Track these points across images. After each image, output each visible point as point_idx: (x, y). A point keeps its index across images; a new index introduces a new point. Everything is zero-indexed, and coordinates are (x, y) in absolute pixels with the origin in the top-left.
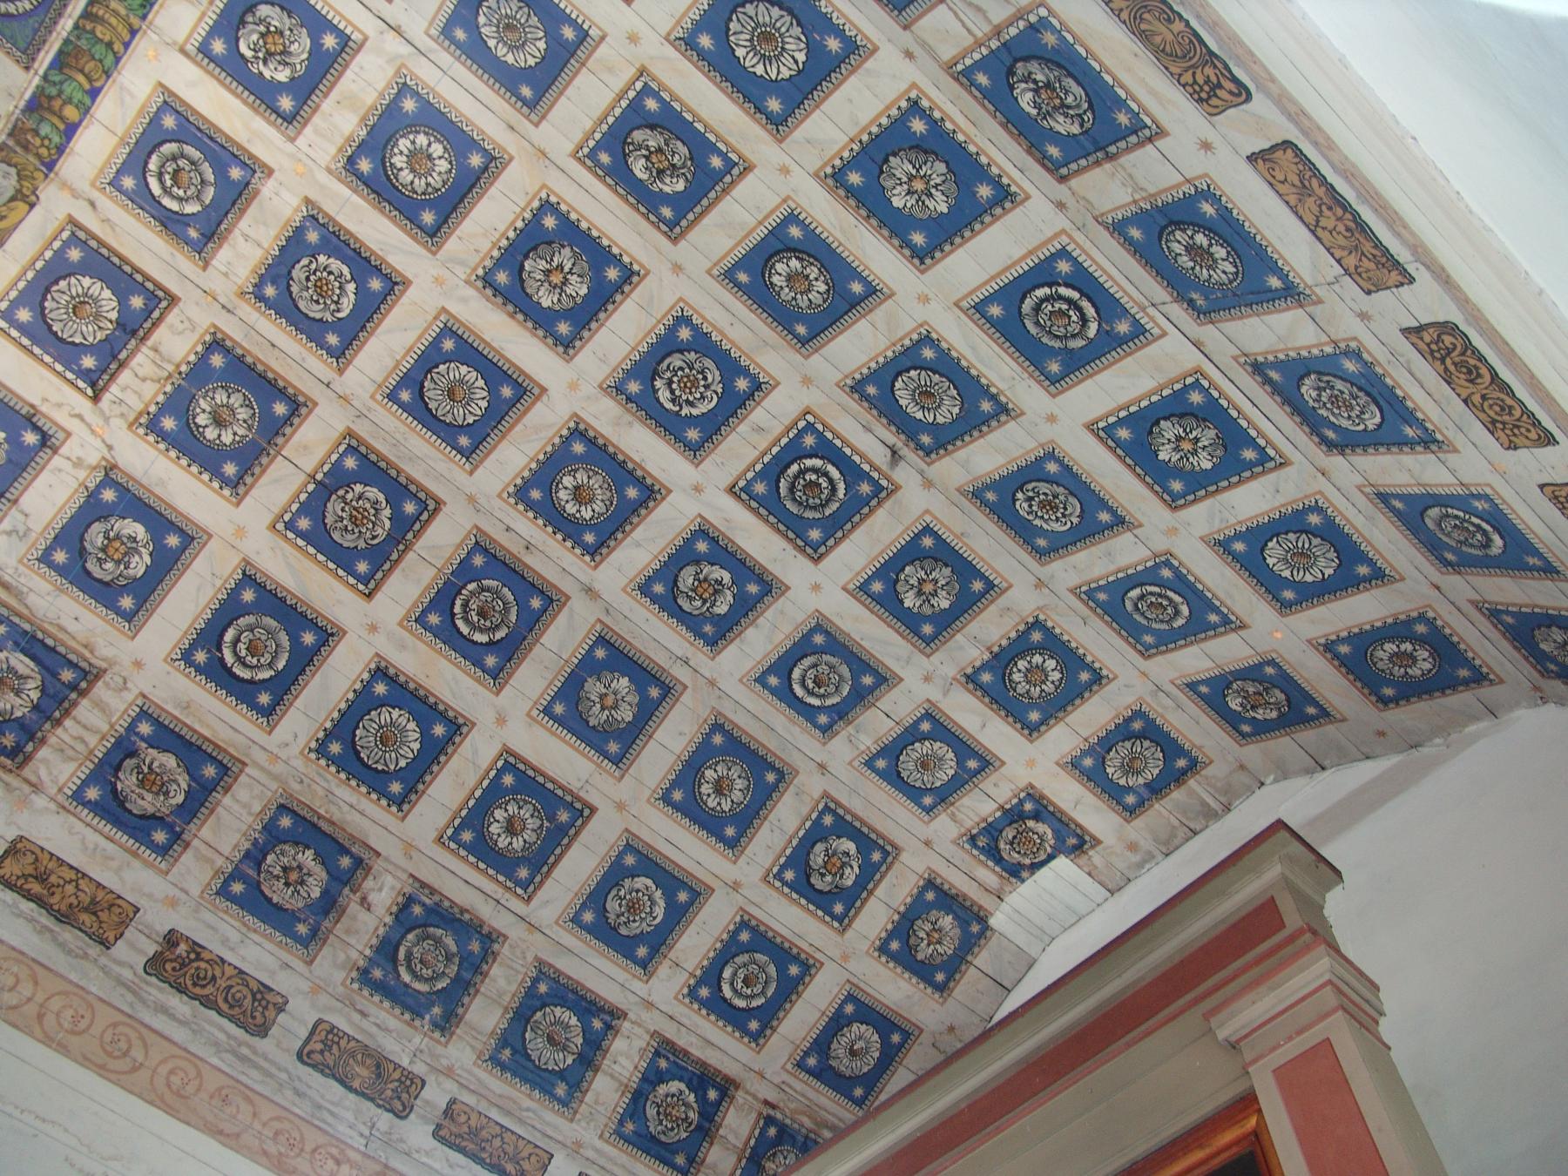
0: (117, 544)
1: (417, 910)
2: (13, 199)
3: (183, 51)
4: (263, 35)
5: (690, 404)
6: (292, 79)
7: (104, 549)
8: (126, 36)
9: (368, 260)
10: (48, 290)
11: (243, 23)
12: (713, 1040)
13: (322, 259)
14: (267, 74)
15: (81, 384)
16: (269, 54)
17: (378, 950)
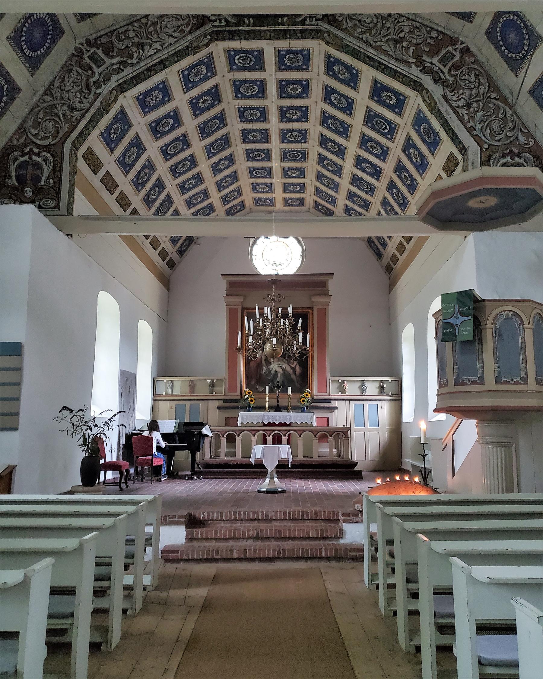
0: (166, 124)
2: (205, 45)
3: (275, 48)
4: (294, 58)
5: (291, 138)
6: (290, 65)
7: (162, 125)
8: (268, 37)
9: (264, 92)
10: (195, 68)
11: (294, 54)
13: (255, 86)
14: (286, 62)
15: (185, 89)
16: (291, 60)
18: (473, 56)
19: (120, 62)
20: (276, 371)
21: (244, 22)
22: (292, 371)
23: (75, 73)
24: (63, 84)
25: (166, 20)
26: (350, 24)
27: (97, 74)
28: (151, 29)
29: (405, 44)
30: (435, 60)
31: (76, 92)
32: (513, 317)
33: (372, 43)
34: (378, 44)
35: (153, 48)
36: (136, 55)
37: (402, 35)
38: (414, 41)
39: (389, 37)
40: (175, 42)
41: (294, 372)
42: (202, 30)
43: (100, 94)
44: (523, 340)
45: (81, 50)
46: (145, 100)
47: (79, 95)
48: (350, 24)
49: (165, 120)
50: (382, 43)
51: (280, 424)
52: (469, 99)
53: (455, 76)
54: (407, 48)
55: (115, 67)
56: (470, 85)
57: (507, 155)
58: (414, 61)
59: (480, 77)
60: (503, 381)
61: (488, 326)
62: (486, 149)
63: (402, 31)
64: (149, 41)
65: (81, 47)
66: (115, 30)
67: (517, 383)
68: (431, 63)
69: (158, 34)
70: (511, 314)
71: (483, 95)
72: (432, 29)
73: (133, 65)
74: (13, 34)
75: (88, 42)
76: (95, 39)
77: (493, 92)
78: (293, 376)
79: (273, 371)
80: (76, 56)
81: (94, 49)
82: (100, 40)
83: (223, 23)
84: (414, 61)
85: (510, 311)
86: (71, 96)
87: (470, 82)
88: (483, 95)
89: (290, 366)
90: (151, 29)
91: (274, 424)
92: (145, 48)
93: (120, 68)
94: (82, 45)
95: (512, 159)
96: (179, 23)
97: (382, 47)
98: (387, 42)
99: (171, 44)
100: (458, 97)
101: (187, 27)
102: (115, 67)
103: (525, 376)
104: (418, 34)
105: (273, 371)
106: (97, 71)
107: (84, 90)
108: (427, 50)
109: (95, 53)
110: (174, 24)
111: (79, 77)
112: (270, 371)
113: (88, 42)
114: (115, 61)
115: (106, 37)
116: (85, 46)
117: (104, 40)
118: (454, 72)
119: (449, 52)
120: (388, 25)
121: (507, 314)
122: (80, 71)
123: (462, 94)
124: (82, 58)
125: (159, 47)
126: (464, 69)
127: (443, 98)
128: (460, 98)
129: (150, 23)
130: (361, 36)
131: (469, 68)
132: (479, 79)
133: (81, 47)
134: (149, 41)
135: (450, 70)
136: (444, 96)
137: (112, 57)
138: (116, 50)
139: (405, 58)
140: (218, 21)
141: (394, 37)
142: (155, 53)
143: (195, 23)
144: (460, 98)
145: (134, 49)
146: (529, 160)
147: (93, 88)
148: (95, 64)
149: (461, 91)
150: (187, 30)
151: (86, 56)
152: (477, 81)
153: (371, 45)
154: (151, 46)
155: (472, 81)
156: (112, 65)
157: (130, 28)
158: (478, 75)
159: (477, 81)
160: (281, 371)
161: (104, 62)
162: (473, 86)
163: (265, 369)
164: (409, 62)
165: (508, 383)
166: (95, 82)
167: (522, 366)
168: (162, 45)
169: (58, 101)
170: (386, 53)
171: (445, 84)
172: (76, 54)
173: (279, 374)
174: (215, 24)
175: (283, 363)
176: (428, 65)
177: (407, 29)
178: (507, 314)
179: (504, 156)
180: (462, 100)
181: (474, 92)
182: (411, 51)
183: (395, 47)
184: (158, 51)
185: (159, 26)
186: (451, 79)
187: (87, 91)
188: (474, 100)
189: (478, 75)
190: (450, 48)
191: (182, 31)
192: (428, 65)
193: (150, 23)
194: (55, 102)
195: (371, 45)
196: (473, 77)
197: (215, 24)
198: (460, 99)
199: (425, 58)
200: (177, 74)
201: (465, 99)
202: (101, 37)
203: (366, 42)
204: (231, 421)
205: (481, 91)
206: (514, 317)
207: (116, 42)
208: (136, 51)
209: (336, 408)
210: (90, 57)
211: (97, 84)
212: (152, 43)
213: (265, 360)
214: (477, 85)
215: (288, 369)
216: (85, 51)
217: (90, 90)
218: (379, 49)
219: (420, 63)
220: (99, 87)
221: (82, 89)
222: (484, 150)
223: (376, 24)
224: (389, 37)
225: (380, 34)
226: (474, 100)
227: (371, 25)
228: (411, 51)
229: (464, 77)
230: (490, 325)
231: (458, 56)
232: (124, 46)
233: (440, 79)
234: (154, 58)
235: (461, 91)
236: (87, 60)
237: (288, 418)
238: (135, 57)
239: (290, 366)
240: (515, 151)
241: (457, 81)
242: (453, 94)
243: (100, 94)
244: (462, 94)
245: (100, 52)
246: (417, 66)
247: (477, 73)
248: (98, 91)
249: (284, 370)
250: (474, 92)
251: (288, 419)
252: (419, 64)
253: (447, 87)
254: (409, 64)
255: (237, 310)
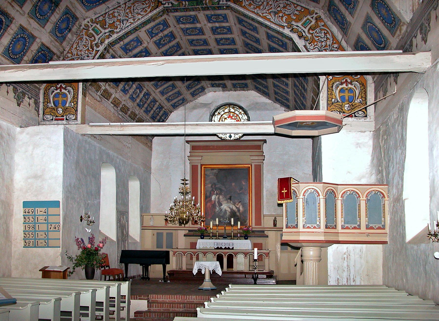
1: (145, 94)
12: (165, 103)
17: (140, 100)
18: (323, 21)
19: (110, 32)
20: (225, 210)
21: (182, 4)
22: (237, 210)
23: (85, 39)
24: (78, 46)
25: (137, 5)
26: (247, 3)
27: (97, 39)
28: (128, 11)
29: (281, 15)
30: (299, 24)
31: (85, 51)
32: (314, 192)
33: (260, 14)
34: (264, 15)
35: (129, 22)
36: (119, 26)
37: (279, 9)
38: (287, 13)
39: (271, 10)
40: (142, 18)
41: (239, 210)
42: (158, 10)
43: (98, 51)
44: (319, 205)
45: (88, 26)
46: (126, 48)
47: (87, 53)
48: (247, 3)
49: (140, 54)
50: (267, 14)
51: (225, 248)
52: (320, 48)
53: (312, 34)
54: (282, 17)
55: (107, 34)
56: (321, 39)
57: (344, 83)
58: (286, 25)
59: (327, 34)
60: (307, 226)
61: (300, 197)
62: (331, 79)
63: (279, 6)
64: (126, 18)
65: (88, 23)
66: (106, 13)
67: (315, 228)
68: (297, 26)
69: (132, 13)
70: (313, 190)
71: (329, 45)
72: (298, 5)
73: (117, 33)
74: (51, 30)
75: (92, 21)
76: (96, 19)
77: (335, 43)
78: (238, 214)
79: (223, 210)
80: (85, 29)
81: (94, 25)
82: (99, 19)
83: (170, 5)
84: (286, 25)
85: (313, 189)
86: (83, 53)
87: (321, 38)
88: (329, 45)
89: (236, 206)
90: (128, 11)
91: (221, 248)
92: (124, 22)
93: (110, 35)
94: (89, 22)
95: (347, 85)
96: (144, 6)
97: (267, 16)
98: (270, 13)
99: (139, 19)
100: (314, 47)
101: (149, 9)
102: (107, 34)
103: (319, 224)
104: (289, 8)
105: (223, 210)
106: (97, 37)
107: (89, 49)
108: (295, 18)
109: (96, 27)
110: (141, 7)
111: (87, 42)
112: (221, 210)
113: (92, 21)
114: (107, 31)
115: (102, 17)
116: (90, 23)
117: (101, 19)
118: (311, 32)
119: (308, 19)
120: (270, 3)
121: (311, 191)
122: (88, 38)
123: (316, 45)
124: (88, 30)
125: (132, 21)
126: (318, 30)
127: (305, 47)
128: (315, 47)
129: (127, 7)
130: (254, 10)
131: (320, 29)
132: (327, 36)
133: (88, 23)
134: (126, 18)
135: (309, 30)
136: (305, 46)
137: (105, 29)
138: (107, 24)
139: (280, 23)
140: (167, 4)
141: (274, 10)
142: (130, 25)
143: (153, 5)
144: (315, 47)
145: (118, 23)
146: (357, 86)
147: (95, 48)
148: (96, 33)
149: (316, 44)
150: (149, 10)
151: (90, 29)
152: (326, 37)
153: (260, 16)
154: (127, 21)
155: (322, 37)
156: (105, 33)
157: (116, 11)
158: (326, 33)
159: (326, 37)
160: (229, 210)
161: (101, 32)
162: (323, 40)
163: (217, 209)
164: (283, 26)
165: (310, 228)
166: (96, 44)
167: (318, 219)
168: (134, 20)
169: (75, 57)
170: (269, 20)
171: (306, 39)
172: (85, 28)
173: (228, 212)
174: (165, 6)
175: (230, 204)
176: (296, 27)
177: (282, 6)
178: (311, 191)
179: (342, 84)
180: (316, 48)
181: (323, 44)
182: (284, 19)
183: (275, 16)
184: (132, 23)
185: (132, 9)
186: (309, 36)
187: (91, 50)
188: (323, 49)
189: (326, 33)
190: (309, 17)
191: (146, 11)
192: (296, 27)
193: (127, 7)
194: (73, 57)
195: (260, 16)
196: (323, 34)
197: (165, 6)
198: (315, 48)
199: (293, 23)
200: (145, 32)
201: (318, 48)
202: (99, 17)
203: (257, 14)
204: (193, 245)
205: (328, 43)
206: (315, 192)
207: (107, 19)
208: (119, 25)
209: (267, 237)
210: (93, 30)
211: (97, 45)
212: (128, 19)
213: (218, 202)
214: (325, 39)
215: (234, 208)
216: (90, 26)
217: (93, 50)
218: (265, 18)
219: (290, 26)
220: (98, 47)
221: (88, 48)
222: (329, 80)
223: (263, 3)
224: (271, 10)
225: (266, 8)
226: (323, 49)
227: (260, 3)
228: (284, 19)
229: (317, 35)
230: (301, 197)
231: (314, 22)
232: (112, 22)
233: (303, 35)
234: (130, 27)
235: (316, 44)
236: (91, 31)
237: (231, 244)
238: (119, 28)
239: (236, 206)
240: (349, 81)
241: (313, 37)
242: (310, 45)
243: (98, 51)
244: (316, 45)
245: (98, 26)
246: (288, 28)
247: (326, 32)
248: (97, 49)
249: (232, 209)
250: (323, 44)
251: (231, 245)
252: (289, 27)
253: (307, 41)
254: (283, 27)
255: (197, 166)
